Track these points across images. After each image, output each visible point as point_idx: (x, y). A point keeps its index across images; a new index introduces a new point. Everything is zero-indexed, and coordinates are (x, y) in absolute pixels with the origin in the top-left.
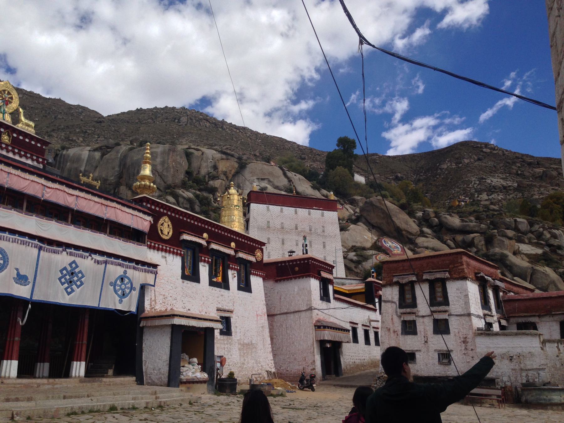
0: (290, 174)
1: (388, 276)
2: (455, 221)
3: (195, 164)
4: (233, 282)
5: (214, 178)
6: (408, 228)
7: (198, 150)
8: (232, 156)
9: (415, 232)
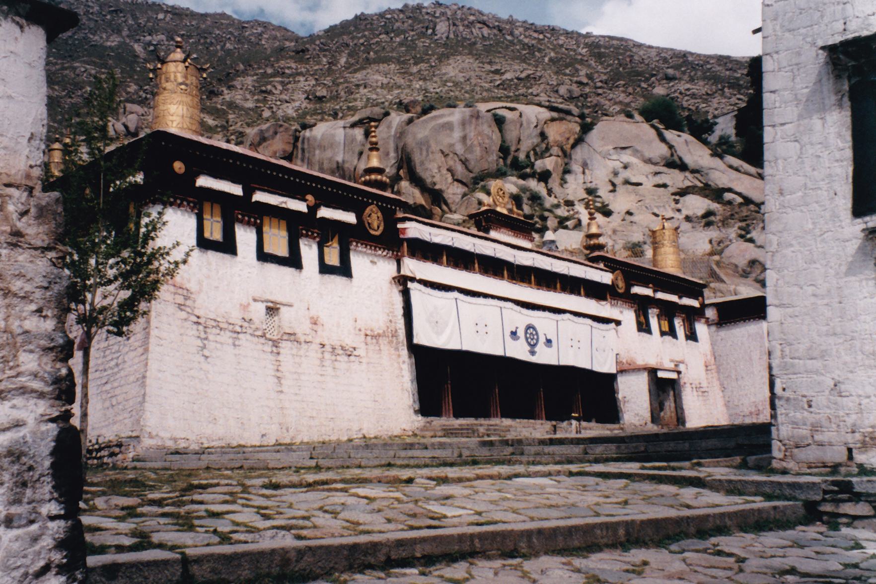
0: (670, 135)
3: (512, 134)
4: (680, 331)
5: (540, 155)
7: (512, 109)
8: (568, 113)
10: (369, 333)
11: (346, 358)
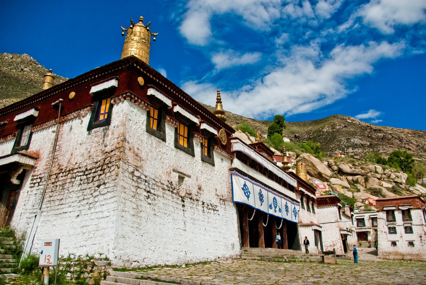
2: (346, 168)
10: (221, 198)
11: (212, 211)
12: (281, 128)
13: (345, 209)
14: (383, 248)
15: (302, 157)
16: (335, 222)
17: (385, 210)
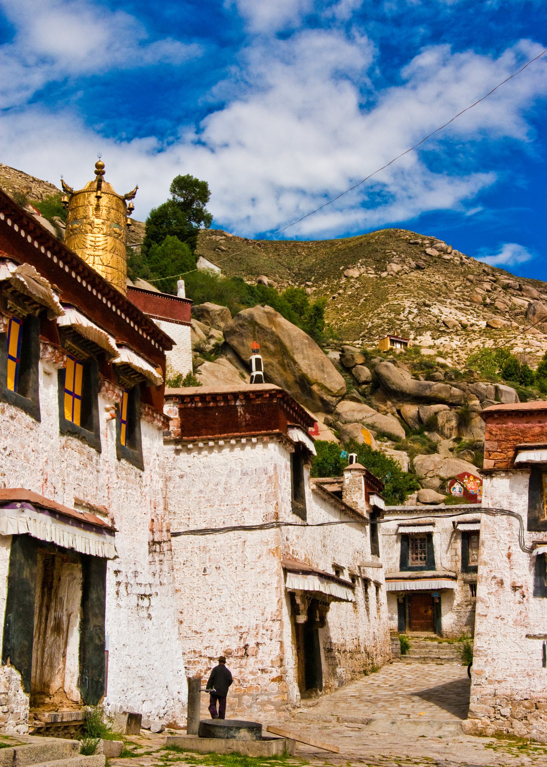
1: (499, 446)
6: (324, 379)
9: (339, 388)
12: (194, 224)
13: (347, 482)
14: (499, 677)
15: (245, 319)
16: (261, 527)
17: (522, 466)
